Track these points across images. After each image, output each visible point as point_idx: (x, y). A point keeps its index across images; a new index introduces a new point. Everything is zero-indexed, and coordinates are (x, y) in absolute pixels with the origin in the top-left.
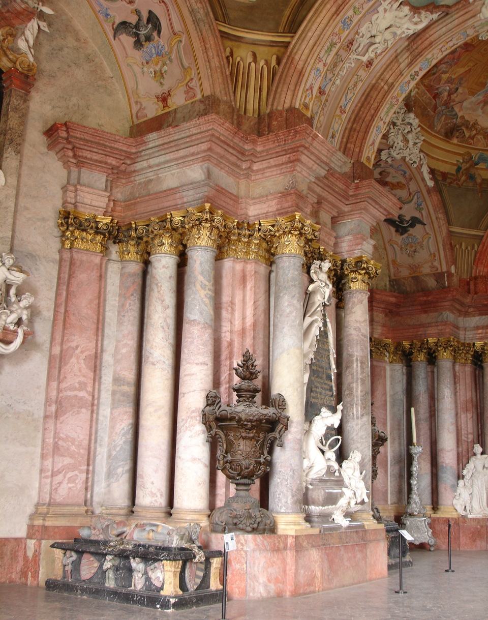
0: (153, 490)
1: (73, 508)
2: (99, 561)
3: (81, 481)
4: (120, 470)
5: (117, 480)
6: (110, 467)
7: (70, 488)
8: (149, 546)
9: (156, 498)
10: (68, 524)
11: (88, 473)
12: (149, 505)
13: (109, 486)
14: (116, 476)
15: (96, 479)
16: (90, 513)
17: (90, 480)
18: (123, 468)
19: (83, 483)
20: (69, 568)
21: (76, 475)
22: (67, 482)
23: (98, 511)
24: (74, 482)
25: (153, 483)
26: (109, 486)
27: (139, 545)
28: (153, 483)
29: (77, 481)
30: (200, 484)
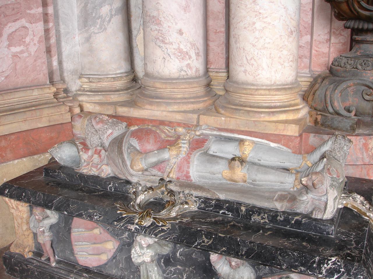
0: (182, 47)
1: (29, 93)
2: (116, 235)
3: (36, 39)
4: (105, 10)
5: (103, 29)
6: (86, 6)
7: (15, 56)
8: (253, 210)
9: (189, 62)
10: (25, 127)
11: (46, 21)
12: (176, 75)
13: (88, 39)
14: (99, 21)
15: (62, 30)
16: (63, 96)
17: (53, 33)
18: (111, 5)
19: (39, 42)
20: (45, 239)
21: (24, 27)
22: (6, 43)
23: (74, 87)
24: (21, 41)
25: (180, 32)
26: (88, 39)
27: (219, 204)
28: (180, 32)
29: (28, 40)
30: (292, 32)
